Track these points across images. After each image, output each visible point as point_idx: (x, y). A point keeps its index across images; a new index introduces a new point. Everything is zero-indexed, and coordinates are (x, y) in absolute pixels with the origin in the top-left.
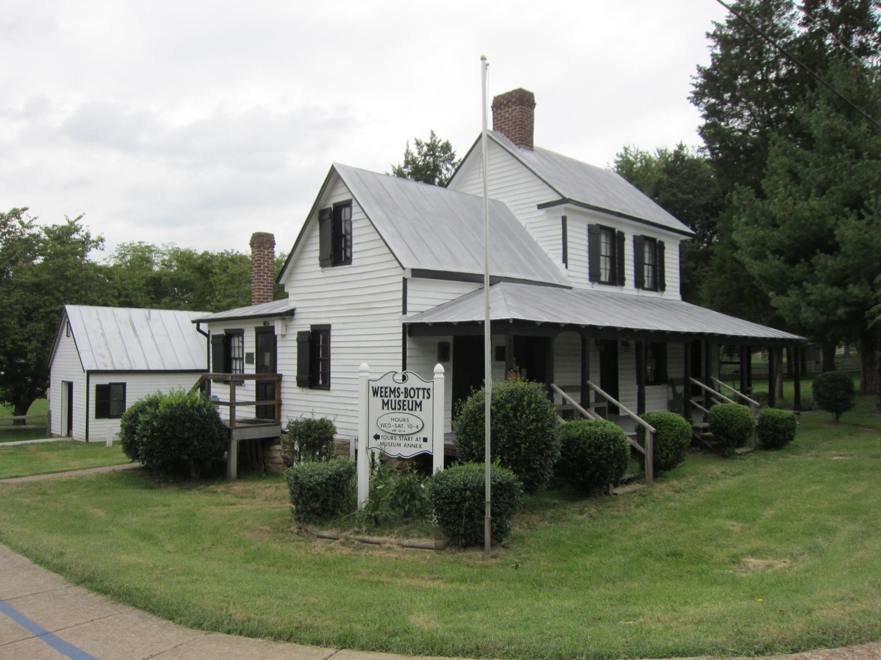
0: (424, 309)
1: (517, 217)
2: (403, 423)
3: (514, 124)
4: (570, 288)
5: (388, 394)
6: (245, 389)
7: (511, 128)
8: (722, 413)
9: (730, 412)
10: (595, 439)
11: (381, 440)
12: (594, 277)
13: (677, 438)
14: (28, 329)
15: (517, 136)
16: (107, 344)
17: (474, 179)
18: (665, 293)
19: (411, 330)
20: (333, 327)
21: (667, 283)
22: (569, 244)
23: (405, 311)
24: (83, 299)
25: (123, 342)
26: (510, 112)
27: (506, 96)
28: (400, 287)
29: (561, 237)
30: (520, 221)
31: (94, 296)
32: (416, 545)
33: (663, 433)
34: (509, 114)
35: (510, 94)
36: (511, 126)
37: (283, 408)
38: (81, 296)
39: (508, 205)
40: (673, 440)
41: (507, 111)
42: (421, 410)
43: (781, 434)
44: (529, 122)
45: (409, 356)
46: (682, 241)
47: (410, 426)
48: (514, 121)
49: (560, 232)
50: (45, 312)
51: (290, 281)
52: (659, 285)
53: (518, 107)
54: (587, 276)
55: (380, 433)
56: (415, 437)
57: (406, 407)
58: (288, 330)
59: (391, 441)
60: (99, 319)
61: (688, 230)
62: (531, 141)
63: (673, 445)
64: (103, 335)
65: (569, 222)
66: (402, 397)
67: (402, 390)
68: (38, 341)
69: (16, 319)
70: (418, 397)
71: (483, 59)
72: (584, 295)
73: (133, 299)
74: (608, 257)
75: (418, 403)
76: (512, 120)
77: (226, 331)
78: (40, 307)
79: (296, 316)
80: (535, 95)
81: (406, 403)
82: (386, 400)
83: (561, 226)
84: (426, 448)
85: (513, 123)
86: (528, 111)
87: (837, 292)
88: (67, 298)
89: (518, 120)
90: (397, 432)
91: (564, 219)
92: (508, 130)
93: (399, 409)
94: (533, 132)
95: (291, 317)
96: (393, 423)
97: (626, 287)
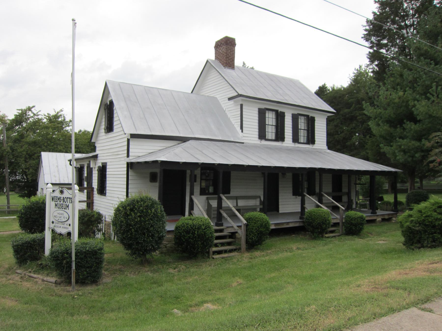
0: (140, 155)
1: (222, 105)
2: (62, 215)
3: (223, 56)
4: (243, 143)
5: (57, 200)
6: (84, 194)
7: (222, 58)
8: (310, 214)
9: (314, 213)
10: (187, 228)
11: (54, 224)
12: (262, 135)
13: (258, 228)
14: (29, 163)
15: (225, 62)
16: (58, 171)
17: (206, 86)
18: (315, 145)
19: (130, 166)
20: (108, 164)
21: (316, 140)
22: (244, 119)
23: (128, 156)
24: (55, 149)
25: (67, 170)
26: (222, 49)
27: (220, 41)
28: (126, 143)
29: (240, 115)
30: (223, 107)
31: (60, 148)
32: (49, 281)
33: (250, 224)
34: (221, 51)
35: (222, 40)
36: (222, 57)
37: (94, 204)
38: (54, 148)
39: (219, 99)
40: (256, 229)
41: (221, 49)
42: (68, 209)
43: (354, 227)
44: (231, 54)
45: (130, 180)
46: (328, 117)
47: (64, 218)
48: (223, 54)
49: (239, 113)
50: (37, 156)
51: (97, 140)
52: (311, 140)
53: (225, 47)
54: (257, 136)
55: (54, 221)
56: (66, 223)
57: (63, 207)
58: (96, 165)
59: (58, 225)
60: (56, 159)
61: (332, 110)
62: (234, 64)
63: (256, 232)
64: (57, 166)
65: (244, 107)
66: (62, 202)
67: (62, 198)
68: (33, 169)
69: (23, 159)
70: (68, 202)
71: (73, 20)
72: (255, 147)
73: (81, 150)
74: (267, 125)
75: (68, 205)
76: (222, 53)
77: (80, 165)
78: (35, 153)
79: (99, 158)
80: (236, 40)
81: (63, 205)
82: (56, 203)
83: (239, 110)
84: (70, 229)
85: (223, 55)
86: (231, 48)
87: (417, 144)
88: (47, 149)
89: (225, 53)
90: (59, 220)
91: (242, 106)
92: (221, 59)
93: (63, 209)
94: (234, 59)
95: (96, 159)
96: (58, 215)
97: (286, 142)
